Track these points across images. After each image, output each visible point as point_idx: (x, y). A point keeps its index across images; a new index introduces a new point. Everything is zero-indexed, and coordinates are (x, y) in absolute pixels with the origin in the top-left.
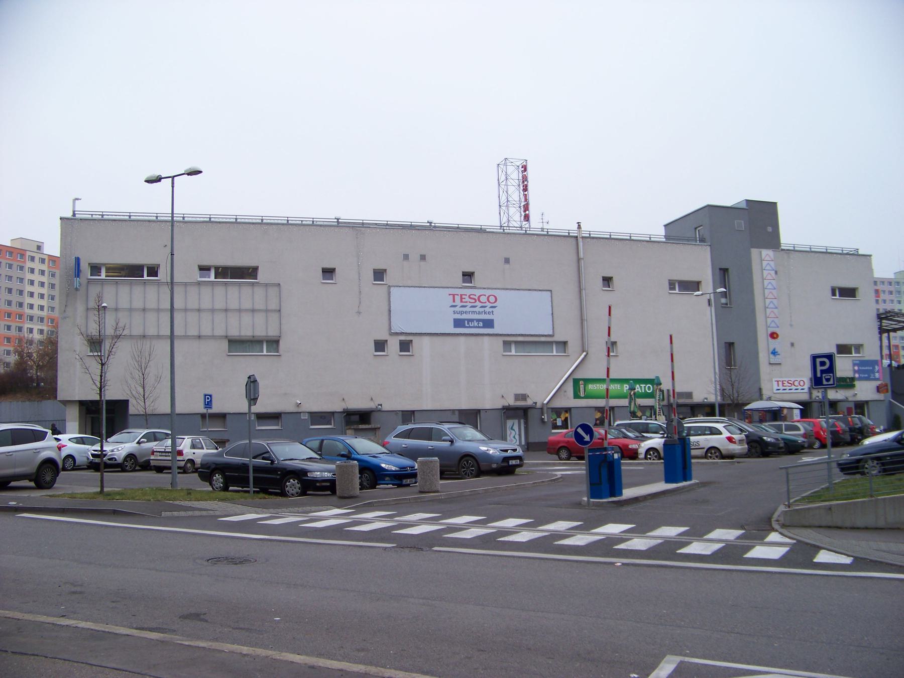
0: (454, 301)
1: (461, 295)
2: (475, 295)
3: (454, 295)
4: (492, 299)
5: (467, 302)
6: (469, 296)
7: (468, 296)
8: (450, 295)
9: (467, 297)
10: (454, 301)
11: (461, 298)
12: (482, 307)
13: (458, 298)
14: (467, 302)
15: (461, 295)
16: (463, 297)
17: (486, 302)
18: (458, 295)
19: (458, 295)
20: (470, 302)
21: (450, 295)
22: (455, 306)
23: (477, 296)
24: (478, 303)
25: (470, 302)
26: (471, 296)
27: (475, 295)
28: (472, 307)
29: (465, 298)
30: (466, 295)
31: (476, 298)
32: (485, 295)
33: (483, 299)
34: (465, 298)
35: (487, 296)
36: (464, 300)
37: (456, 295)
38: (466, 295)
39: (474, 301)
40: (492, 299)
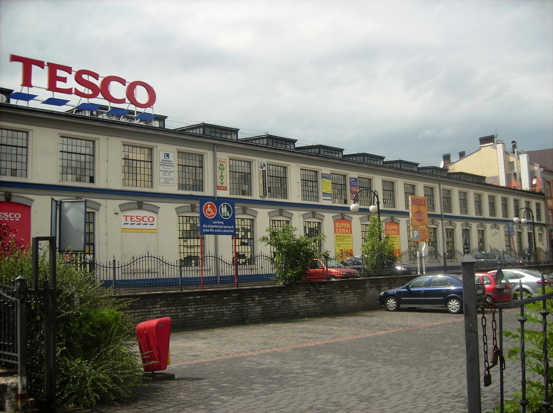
0: (126, 220)
1: (131, 216)
2: (140, 217)
3: (126, 216)
4: (151, 219)
5: (135, 221)
8: (124, 216)
9: (135, 218)
10: (126, 220)
11: (131, 219)
13: (129, 218)
14: (135, 221)
16: (133, 217)
17: (147, 221)
18: (129, 216)
19: (129, 216)
20: (136, 221)
21: (124, 216)
22: (127, 224)
23: (142, 217)
24: (142, 222)
25: (136, 221)
26: (138, 217)
27: (140, 217)
28: (138, 224)
29: (133, 219)
30: (134, 216)
31: (141, 218)
32: (147, 217)
33: (145, 219)
34: (133, 219)
36: (133, 220)
38: (134, 216)
39: (139, 220)
40: (151, 219)
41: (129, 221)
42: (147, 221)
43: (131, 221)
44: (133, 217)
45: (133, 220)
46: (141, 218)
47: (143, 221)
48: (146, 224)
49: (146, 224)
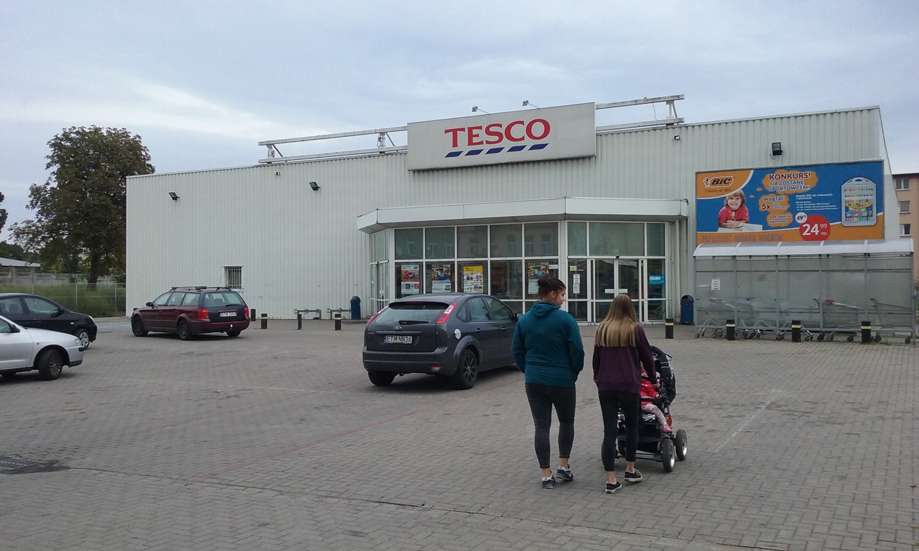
0: (455, 144)
1: (470, 129)
2: (500, 126)
3: (455, 132)
4: (538, 130)
5: (481, 143)
8: (447, 131)
10: (455, 144)
11: (471, 136)
12: (513, 149)
13: (463, 137)
14: (481, 143)
15: (470, 129)
16: (475, 132)
17: (523, 139)
18: (463, 130)
19: (463, 130)
20: (488, 142)
21: (447, 131)
22: (457, 154)
24: (506, 144)
25: (488, 142)
26: (491, 129)
27: (500, 126)
28: (491, 151)
29: (477, 136)
30: (480, 128)
31: (502, 130)
32: (522, 123)
33: (518, 131)
34: (477, 136)
35: (526, 124)
38: (480, 128)
39: (496, 138)
40: (538, 130)
41: (463, 145)
42: (523, 139)
43: (470, 143)
44: (475, 132)
45: (475, 140)
46: (502, 130)
47: (510, 138)
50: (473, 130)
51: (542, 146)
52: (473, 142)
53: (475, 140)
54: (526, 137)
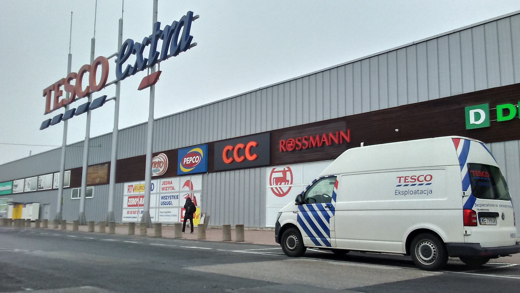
0: (400, 182)
1: (406, 177)
2: (416, 176)
3: (400, 177)
4: (428, 178)
5: (409, 182)
6: (411, 177)
7: (410, 177)
9: (409, 178)
10: (400, 182)
11: (405, 179)
13: (403, 180)
14: (409, 182)
17: (423, 181)
18: (403, 177)
19: (403, 177)
20: (411, 182)
24: (417, 183)
25: (411, 182)
26: (412, 177)
27: (416, 176)
29: (407, 179)
30: (409, 177)
31: (416, 178)
32: (423, 176)
34: (407, 179)
35: (425, 176)
37: (402, 177)
38: (409, 177)
39: (414, 180)
40: (428, 178)
42: (423, 181)
43: (405, 182)
45: (407, 181)
46: (416, 178)
48: (422, 184)
49: (422, 184)
50: (407, 178)
51: (430, 184)
52: (406, 181)
53: (407, 181)
54: (424, 181)
